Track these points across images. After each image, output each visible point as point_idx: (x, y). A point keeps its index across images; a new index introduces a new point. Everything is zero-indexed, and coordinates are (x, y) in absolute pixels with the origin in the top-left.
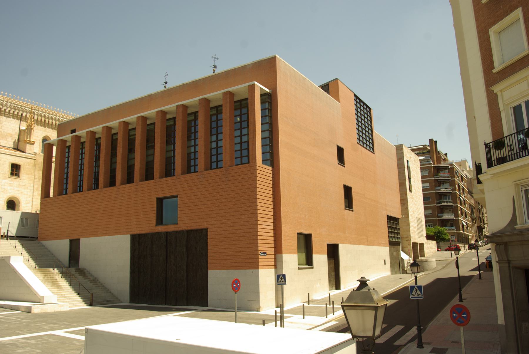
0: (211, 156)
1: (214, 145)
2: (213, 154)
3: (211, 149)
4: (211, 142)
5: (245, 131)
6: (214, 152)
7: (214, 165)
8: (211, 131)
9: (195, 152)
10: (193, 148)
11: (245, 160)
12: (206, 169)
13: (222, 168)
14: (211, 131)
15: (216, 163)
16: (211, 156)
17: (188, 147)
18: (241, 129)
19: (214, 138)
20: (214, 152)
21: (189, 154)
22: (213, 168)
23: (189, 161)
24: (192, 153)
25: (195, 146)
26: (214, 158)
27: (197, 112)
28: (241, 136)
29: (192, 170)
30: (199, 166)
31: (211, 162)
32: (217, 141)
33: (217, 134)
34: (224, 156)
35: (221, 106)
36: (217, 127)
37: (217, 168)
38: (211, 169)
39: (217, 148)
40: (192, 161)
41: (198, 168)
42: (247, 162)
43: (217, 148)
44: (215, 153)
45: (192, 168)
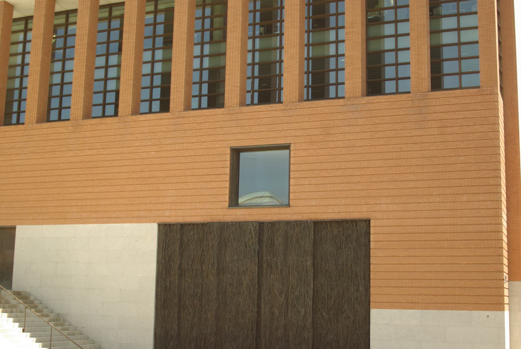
0: (50, 97)
1: (57, 79)
2: (54, 94)
3: (51, 86)
4: (52, 73)
5: (113, 60)
6: (56, 91)
7: (54, 115)
8: (53, 55)
9: (21, 88)
10: (17, 81)
11: (110, 110)
12: (40, 121)
13: (69, 120)
14: (53, 55)
15: (57, 111)
16: (50, 97)
17: (9, 78)
18: (107, 55)
19: (58, 66)
20: (56, 91)
21: (10, 91)
22: (51, 119)
23: (9, 103)
24: (17, 89)
25: (22, 76)
26: (55, 103)
27: (31, 17)
28: (107, 67)
29: (14, 120)
30: (27, 114)
31: (49, 110)
32: (63, 72)
33: (64, 60)
34: (73, 99)
35: (75, 11)
36: (65, 48)
37: (60, 119)
38: (48, 121)
39: (62, 84)
40: (15, 105)
41: (24, 118)
42: (113, 114)
43: (62, 84)
44: (58, 93)
45: (15, 116)
